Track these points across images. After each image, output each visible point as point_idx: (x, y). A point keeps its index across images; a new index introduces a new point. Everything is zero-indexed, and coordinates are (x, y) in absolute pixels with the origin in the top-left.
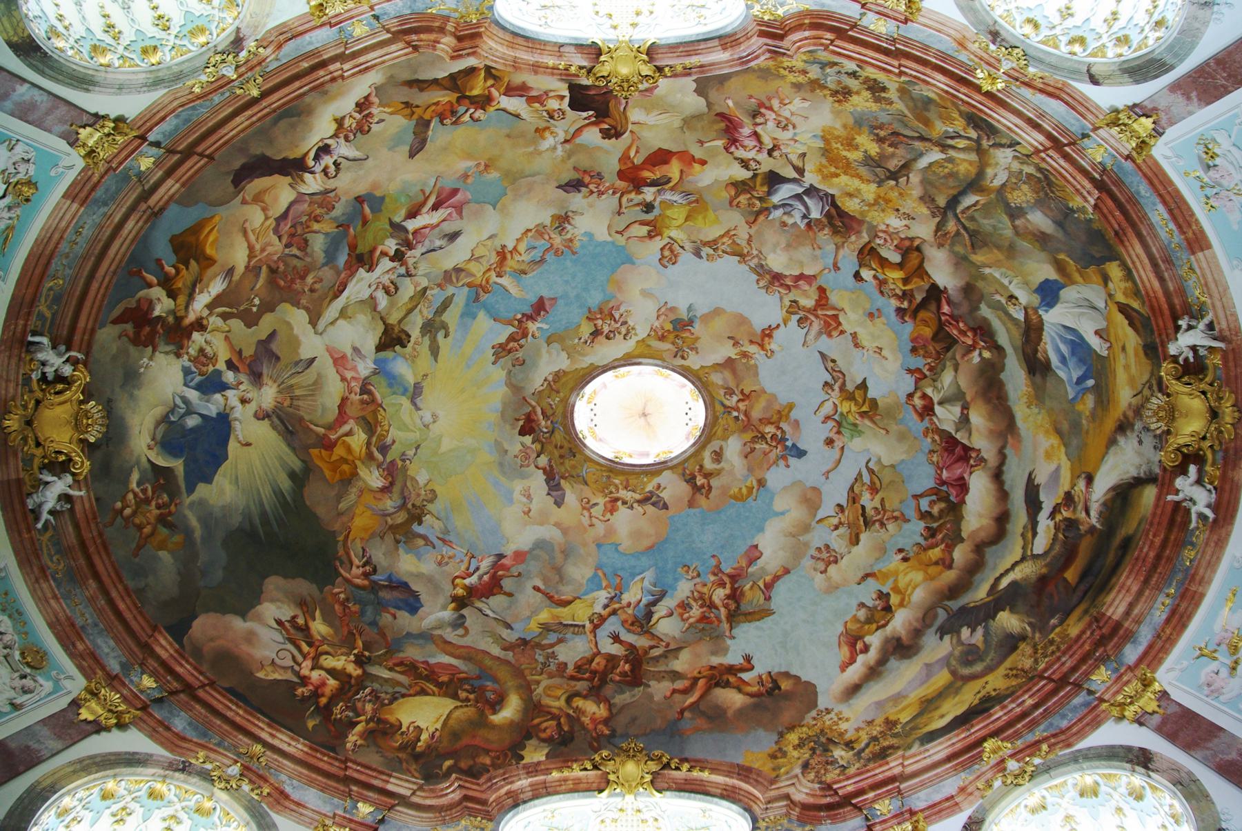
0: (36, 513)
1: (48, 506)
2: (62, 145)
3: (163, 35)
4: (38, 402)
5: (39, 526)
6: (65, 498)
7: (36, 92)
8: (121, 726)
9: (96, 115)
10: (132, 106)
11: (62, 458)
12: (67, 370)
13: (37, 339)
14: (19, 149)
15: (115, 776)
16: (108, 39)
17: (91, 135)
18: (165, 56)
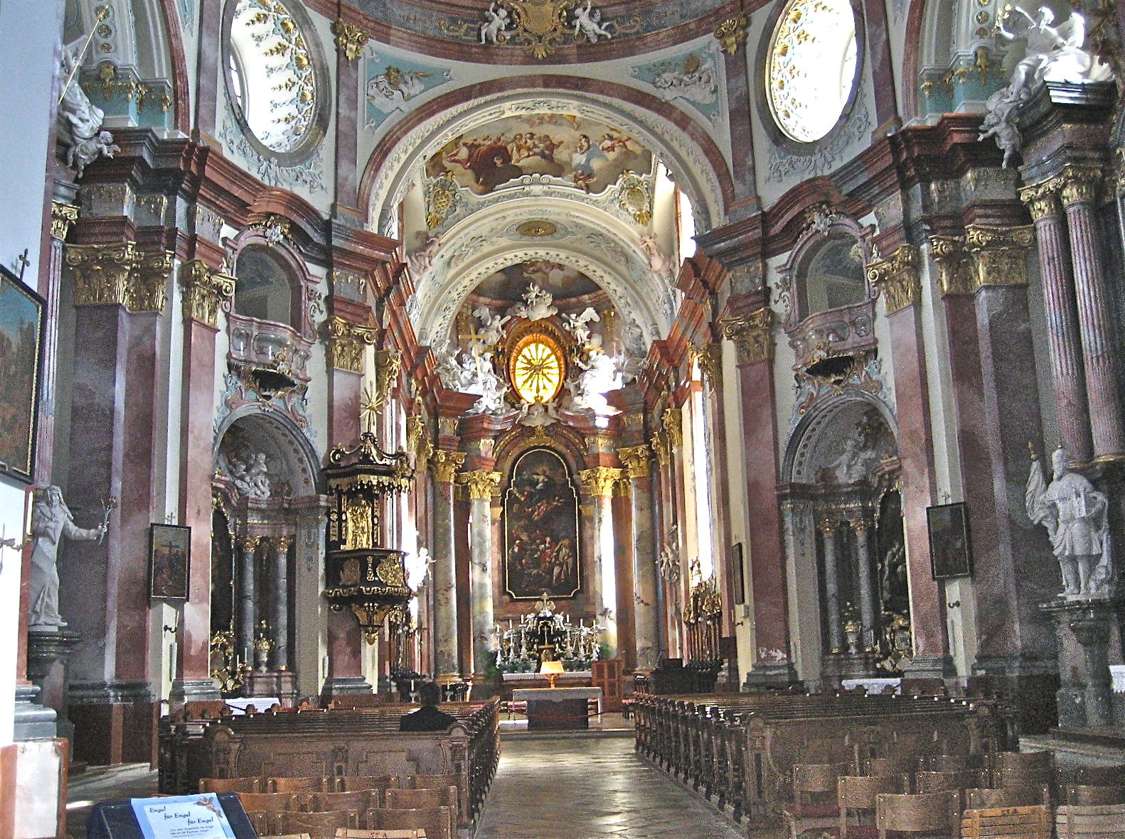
0: (599, 36)
1: (596, 27)
2: (361, 62)
3: (270, 18)
4: (525, 30)
5: (609, 36)
6: (591, 15)
7: (340, 102)
8: (748, 23)
9: (337, 50)
10: (322, 24)
11: (565, 14)
12: (503, 13)
13: (483, 37)
14: (371, 92)
15: (773, 48)
16: (288, 53)
17: (351, 49)
18: (286, 17)
